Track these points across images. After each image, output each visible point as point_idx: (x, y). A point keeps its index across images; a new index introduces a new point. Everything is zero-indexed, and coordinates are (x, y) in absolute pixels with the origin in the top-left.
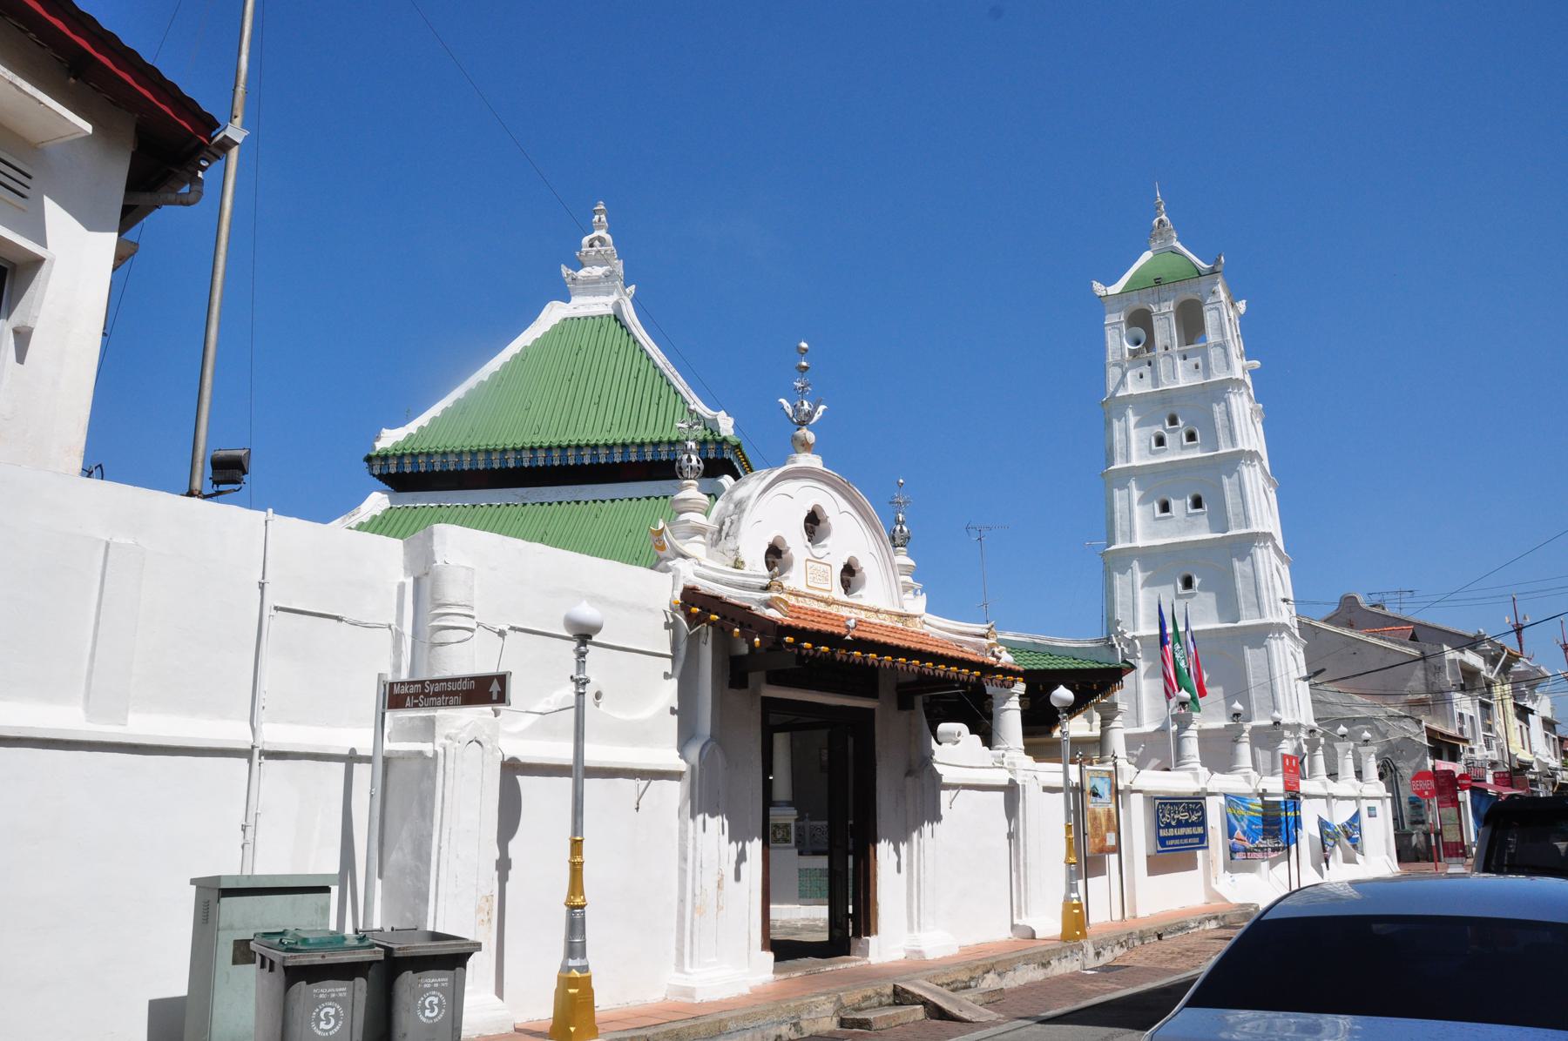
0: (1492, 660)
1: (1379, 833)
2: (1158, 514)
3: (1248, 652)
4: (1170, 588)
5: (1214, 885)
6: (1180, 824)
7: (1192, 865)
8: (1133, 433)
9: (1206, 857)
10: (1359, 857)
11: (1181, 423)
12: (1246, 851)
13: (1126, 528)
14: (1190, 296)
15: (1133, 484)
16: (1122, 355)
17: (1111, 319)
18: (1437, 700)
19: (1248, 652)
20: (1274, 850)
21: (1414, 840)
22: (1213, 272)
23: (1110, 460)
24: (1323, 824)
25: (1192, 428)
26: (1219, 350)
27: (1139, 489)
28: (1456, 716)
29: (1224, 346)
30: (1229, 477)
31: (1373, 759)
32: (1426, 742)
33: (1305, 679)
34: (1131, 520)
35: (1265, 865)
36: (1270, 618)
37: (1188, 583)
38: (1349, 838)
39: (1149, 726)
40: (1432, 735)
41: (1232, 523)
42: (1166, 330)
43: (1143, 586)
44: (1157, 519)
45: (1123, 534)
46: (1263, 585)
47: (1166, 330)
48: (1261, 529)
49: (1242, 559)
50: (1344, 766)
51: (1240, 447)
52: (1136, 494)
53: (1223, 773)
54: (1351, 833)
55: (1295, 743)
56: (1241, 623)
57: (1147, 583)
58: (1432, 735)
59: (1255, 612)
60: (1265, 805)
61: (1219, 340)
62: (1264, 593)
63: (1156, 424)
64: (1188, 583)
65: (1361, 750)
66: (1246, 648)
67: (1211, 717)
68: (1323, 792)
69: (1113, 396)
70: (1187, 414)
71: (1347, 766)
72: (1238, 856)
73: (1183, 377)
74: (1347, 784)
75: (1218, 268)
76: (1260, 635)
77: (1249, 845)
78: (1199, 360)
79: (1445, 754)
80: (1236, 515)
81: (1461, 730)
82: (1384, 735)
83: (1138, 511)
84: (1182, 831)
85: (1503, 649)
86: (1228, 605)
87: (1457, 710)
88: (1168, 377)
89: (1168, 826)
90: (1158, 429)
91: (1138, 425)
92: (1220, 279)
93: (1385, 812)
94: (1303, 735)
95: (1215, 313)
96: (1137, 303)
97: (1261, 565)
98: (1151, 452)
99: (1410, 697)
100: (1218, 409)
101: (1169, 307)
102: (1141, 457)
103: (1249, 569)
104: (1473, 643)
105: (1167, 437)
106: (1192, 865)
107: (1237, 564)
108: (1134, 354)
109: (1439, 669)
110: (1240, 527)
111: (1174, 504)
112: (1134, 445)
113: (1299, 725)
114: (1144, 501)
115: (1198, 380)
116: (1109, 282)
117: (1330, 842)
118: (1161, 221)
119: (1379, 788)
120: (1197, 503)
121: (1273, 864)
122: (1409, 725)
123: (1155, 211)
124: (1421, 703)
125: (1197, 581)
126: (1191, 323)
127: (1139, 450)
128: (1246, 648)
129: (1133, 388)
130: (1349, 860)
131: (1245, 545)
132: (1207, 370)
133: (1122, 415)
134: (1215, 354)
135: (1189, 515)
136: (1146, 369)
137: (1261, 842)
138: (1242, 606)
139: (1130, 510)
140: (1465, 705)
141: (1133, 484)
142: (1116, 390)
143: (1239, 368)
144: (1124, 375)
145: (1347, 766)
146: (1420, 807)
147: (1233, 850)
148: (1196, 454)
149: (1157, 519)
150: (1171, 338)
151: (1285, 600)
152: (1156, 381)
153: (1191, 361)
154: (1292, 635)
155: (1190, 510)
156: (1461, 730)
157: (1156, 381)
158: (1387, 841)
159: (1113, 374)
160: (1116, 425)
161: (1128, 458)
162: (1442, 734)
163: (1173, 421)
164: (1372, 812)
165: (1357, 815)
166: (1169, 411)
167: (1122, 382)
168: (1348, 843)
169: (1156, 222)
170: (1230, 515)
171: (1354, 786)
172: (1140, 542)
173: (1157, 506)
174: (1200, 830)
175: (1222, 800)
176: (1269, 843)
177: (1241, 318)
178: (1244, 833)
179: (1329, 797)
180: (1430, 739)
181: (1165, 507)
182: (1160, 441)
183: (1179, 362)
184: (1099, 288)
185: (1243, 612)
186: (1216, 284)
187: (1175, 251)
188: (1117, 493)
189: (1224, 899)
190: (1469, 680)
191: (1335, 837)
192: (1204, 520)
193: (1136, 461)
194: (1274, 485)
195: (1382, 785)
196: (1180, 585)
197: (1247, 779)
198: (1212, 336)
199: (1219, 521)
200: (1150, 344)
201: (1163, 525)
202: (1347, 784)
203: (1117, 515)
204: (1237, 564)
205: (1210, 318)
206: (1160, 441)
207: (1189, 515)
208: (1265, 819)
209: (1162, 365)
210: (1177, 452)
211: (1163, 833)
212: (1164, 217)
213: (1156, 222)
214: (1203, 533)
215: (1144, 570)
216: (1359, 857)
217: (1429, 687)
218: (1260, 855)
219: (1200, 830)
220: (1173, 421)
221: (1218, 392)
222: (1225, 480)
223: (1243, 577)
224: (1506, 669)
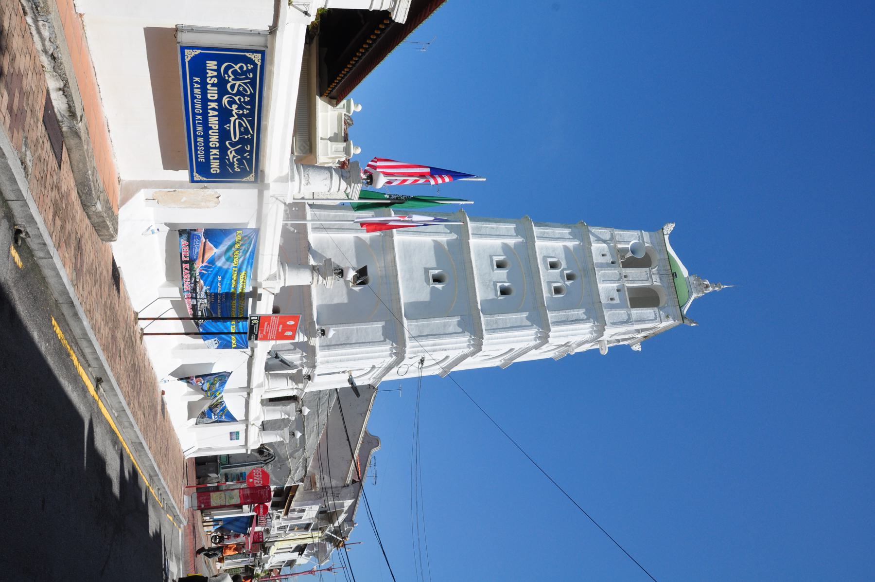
0: (337, 531)
1: (214, 440)
2: (495, 259)
3: (379, 325)
4: (434, 265)
5: (142, 194)
6: (224, 115)
7: (170, 163)
8: (559, 244)
9: (181, 185)
10: (193, 421)
11: (568, 283)
12: (191, 262)
13: (483, 231)
14: (663, 300)
15: (520, 240)
16: (620, 242)
17: (646, 235)
18: (315, 494)
19: (379, 325)
20: (194, 307)
21: (213, 475)
22: (683, 318)
23: (539, 224)
24: (223, 377)
25: (565, 291)
26: (625, 318)
27: (516, 245)
28: (303, 508)
29: (628, 321)
30: (528, 318)
31: (279, 439)
32: (287, 485)
33: (351, 381)
34: (490, 236)
35: (175, 293)
36: (410, 345)
37: (437, 279)
38: (211, 409)
39: (313, 238)
40: (292, 490)
41: (489, 318)
42: (638, 278)
43: (435, 242)
44: (491, 257)
45: (479, 228)
46: (438, 341)
47: (638, 278)
48: (485, 342)
49: (459, 324)
50: (274, 411)
51: (553, 329)
52: (511, 242)
53: (281, 249)
54: (213, 412)
55: (298, 363)
56: (405, 321)
57: (437, 246)
58: (292, 490)
59: (415, 333)
60: (243, 296)
61: (634, 317)
62: (430, 342)
63: (568, 263)
64: (437, 279)
65: (286, 431)
66: (383, 323)
67: (324, 292)
68: (254, 384)
69: (589, 231)
70: (577, 289)
71: (276, 414)
72: (184, 242)
73: (606, 287)
74: (259, 414)
75: (686, 322)
76: (394, 335)
77: (198, 266)
78: (617, 301)
79: (277, 499)
80: (496, 322)
81: (294, 510)
82: (292, 456)
83: (498, 242)
84: (214, 122)
85: (344, 538)
86: (420, 311)
87: (307, 508)
88: (604, 275)
89: (221, 85)
90: (564, 265)
91: (566, 248)
92: (677, 323)
93: (233, 448)
94: (305, 371)
95: (652, 316)
96: (656, 257)
97: (454, 340)
98: (545, 258)
99: (317, 477)
100: (580, 313)
101: (656, 282)
102: (541, 248)
103: (451, 329)
104: (349, 520)
105: (556, 272)
106: (170, 163)
107: (455, 320)
108: (623, 251)
109: (336, 496)
110: (487, 324)
111: (503, 273)
112: (552, 243)
113: (314, 367)
114: (506, 248)
115: (603, 300)
116: (671, 236)
117: (206, 386)
118: (707, 287)
119: (254, 445)
120: (504, 292)
121: (176, 305)
122: (299, 474)
123: (714, 282)
124: (313, 484)
125: (439, 286)
126: (643, 298)
127: (547, 248)
128: (383, 323)
129: (597, 248)
130: (191, 406)
131: (472, 327)
132: (612, 307)
133: (574, 236)
134: (622, 313)
135: (495, 283)
136: (609, 259)
137: (203, 288)
138: (421, 323)
139: (498, 236)
140: (311, 513)
141: (520, 240)
142: (593, 234)
143: (612, 334)
144: (604, 241)
145: (276, 414)
146: (239, 480)
147: (188, 233)
148: (546, 294)
149: (491, 257)
150: (633, 281)
151: (422, 361)
152: (602, 266)
153: (616, 295)
154: (389, 368)
155: (499, 285)
156: (294, 510)
157: (602, 266)
158: (210, 449)
159: (605, 233)
160: (566, 231)
161: (542, 238)
162: (293, 496)
163: (570, 277)
164: (234, 435)
165: (231, 419)
166: (577, 274)
167: (599, 240)
168: (205, 408)
169: (707, 282)
170: (496, 317)
171: (257, 418)
172: (473, 242)
173: (501, 258)
174: (215, 166)
175: (252, 225)
176: (203, 303)
177: (628, 347)
178: (212, 261)
179: (248, 390)
180: (290, 488)
181: (500, 265)
182: (553, 266)
183: (615, 285)
184: (669, 228)
185: (414, 323)
186: (674, 319)
187: (690, 294)
188: (512, 226)
189: (124, 201)
190: (326, 516)
191: (211, 393)
192: (491, 296)
193: (538, 244)
194: (504, 365)
195: (257, 446)
196: (436, 272)
197: (273, 277)
198: (636, 312)
199: (491, 308)
200: (630, 263)
201: (486, 262)
202: (259, 414)
203: (494, 225)
204: (455, 320)
205: (649, 312)
206: (553, 266)
207: (495, 283)
208: (229, 296)
209: (614, 272)
210: (547, 278)
211: (211, 64)
212: (711, 289)
213: (707, 282)
214: (481, 294)
215: (448, 243)
216: (193, 421)
217: (324, 489)
218: (188, 286)
219: (215, 166)
220: (570, 277)
221: (595, 313)
222: (525, 315)
223: (445, 325)
224: (330, 539)
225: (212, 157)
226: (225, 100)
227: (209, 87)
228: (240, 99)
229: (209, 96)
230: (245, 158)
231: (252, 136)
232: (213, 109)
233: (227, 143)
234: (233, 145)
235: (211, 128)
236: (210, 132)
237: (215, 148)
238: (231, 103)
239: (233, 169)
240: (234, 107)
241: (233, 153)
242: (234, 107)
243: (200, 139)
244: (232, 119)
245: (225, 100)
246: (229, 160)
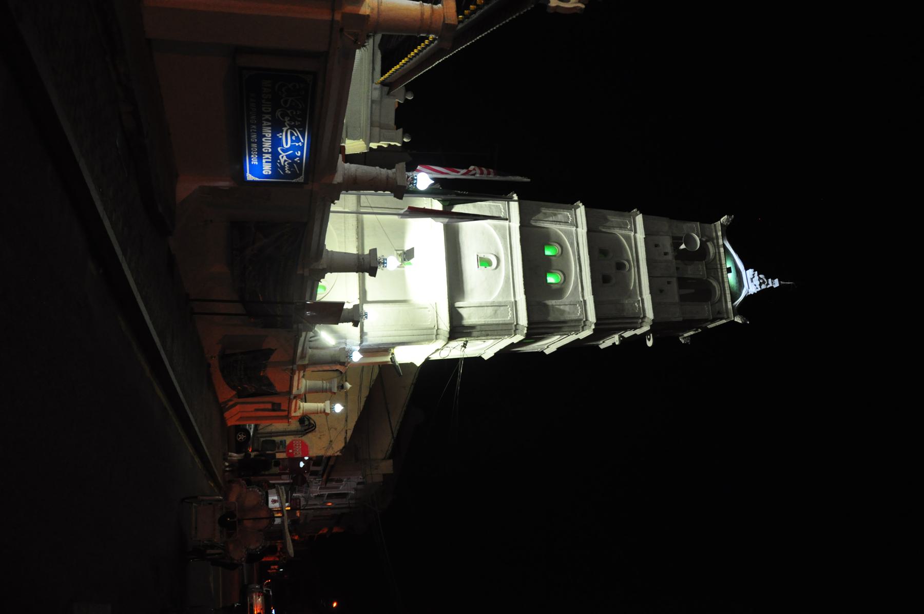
225: (264, 161)
226: (278, 114)
227: (263, 101)
228: (292, 113)
229: (263, 109)
230: (296, 162)
231: (303, 144)
232: (267, 120)
233: (279, 149)
234: (284, 151)
235: (265, 136)
236: (264, 139)
237: (268, 153)
238: (283, 115)
239: (284, 170)
240: (287, 119)
241: (285, 158)
242: (287, 119)
243: (254, 145)
244: (285, 129)
245: (278, 114)
246: (280, 163)
